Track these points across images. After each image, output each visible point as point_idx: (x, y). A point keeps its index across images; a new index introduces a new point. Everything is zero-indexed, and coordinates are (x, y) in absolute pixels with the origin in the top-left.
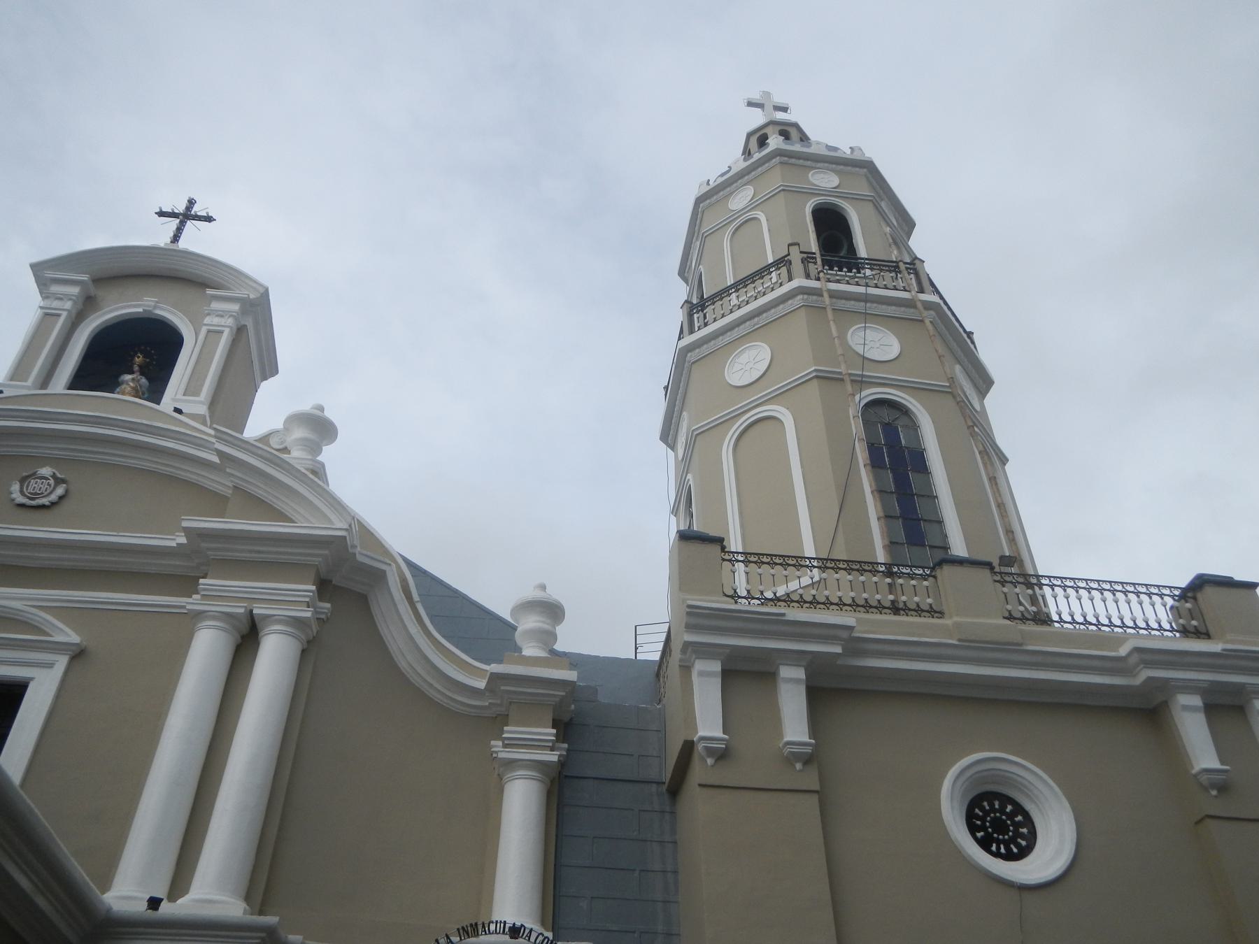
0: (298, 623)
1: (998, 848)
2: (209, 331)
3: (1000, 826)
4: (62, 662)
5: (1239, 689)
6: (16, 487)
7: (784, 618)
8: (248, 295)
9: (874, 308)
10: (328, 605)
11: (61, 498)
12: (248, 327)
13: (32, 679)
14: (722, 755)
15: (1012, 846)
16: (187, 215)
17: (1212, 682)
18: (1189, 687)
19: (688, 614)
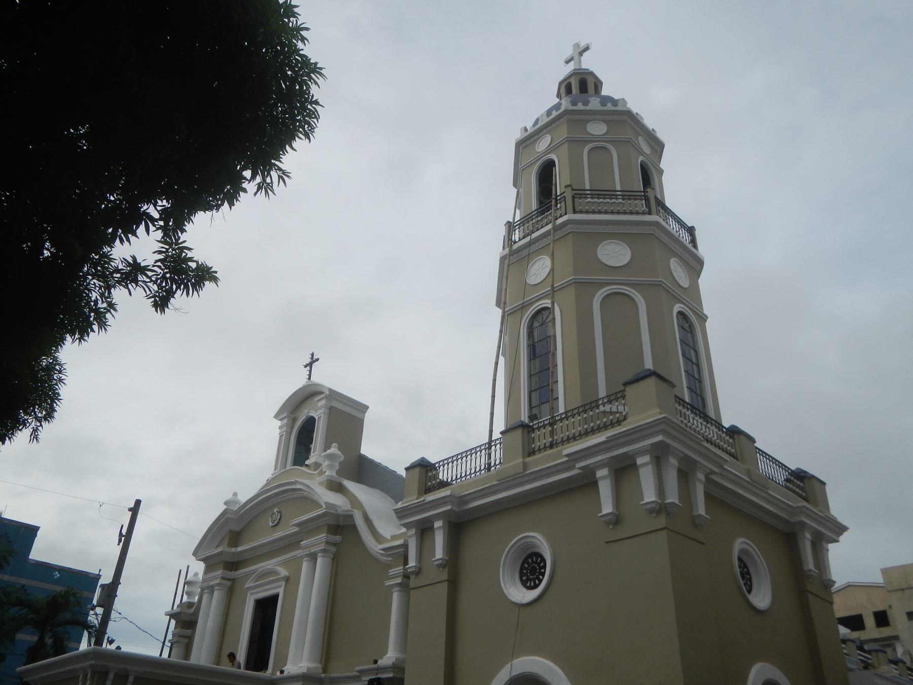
0: (324, 551)
1: (531, 584)
2: (319, 418)
3: (533, 571)
4: (283, 583)
5: (626, 456)
6: (270, 520)
7: (426, 501)
8: (326, 394)
9: (533, 248)
10: (338, 537)
11: (280, 519)
13: (279, 592)
14: (418, 572)
18: (600, 465)
19: (396, 513)
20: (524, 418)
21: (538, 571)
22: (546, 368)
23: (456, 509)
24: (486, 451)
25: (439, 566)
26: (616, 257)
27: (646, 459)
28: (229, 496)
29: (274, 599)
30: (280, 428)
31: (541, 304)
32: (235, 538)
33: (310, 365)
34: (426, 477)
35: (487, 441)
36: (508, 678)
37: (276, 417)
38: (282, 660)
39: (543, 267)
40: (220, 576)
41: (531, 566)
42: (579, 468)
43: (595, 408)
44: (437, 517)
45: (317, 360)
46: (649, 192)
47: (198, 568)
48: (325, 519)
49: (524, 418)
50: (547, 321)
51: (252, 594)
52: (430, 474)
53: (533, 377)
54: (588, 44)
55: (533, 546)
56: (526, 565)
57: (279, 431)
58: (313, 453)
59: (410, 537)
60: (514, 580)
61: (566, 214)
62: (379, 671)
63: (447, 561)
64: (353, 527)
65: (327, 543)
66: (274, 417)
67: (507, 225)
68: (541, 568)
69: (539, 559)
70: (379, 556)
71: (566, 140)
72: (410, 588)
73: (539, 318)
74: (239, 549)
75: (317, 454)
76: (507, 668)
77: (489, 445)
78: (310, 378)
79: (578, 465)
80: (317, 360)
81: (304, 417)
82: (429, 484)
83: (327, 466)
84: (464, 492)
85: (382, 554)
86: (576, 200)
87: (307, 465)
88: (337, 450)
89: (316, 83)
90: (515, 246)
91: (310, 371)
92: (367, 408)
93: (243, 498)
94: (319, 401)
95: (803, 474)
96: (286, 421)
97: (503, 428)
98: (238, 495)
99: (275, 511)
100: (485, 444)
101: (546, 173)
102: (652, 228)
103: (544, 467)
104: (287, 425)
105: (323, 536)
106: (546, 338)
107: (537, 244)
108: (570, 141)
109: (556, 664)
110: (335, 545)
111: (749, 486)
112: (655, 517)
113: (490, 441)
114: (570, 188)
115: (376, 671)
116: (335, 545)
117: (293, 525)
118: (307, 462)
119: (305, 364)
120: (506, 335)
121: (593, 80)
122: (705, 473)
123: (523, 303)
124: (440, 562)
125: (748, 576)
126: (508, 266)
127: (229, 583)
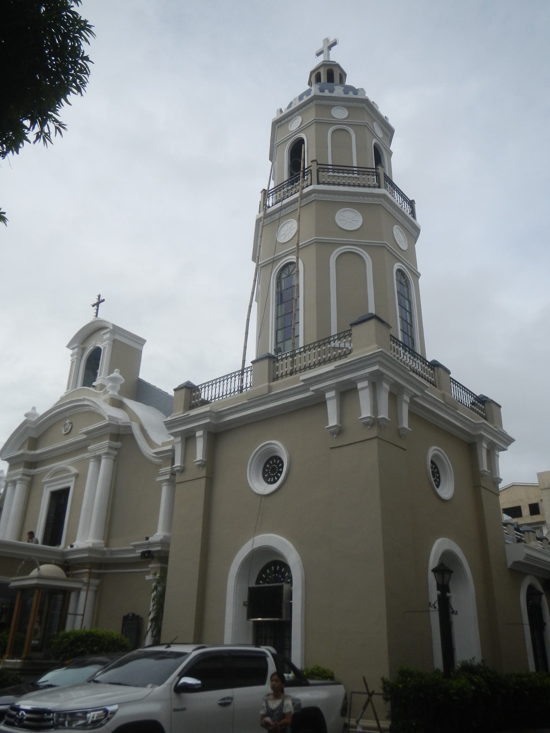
0: (107, 454)
1: (271, 479)
2: (104, 348)
3: (273, 470)
4: (74, 479)
6: (63, 429)
8: (110, 329)
9: (284, 212)
10: (119, 443)
11: (71, 429)
12: (117, 338)
14: (182, 470)
15: (276, 477)
16: (100, 301)
17: (337, 383)
18: (329, 389)
19: (165, 424)
20: (271, 351)
21: (277, 470)
22: (290, 312)
23: (215, 422)
24: (239, 376)
25: (199, 466)
26: (350, 222)
27: (365, 384)
28: (29, 410)
30: (72, 355)
31: (288, 259)
32: (34, 443)
33: (97, 304)
34: (191, 396)
35: (241, 369)
36: (250, 550)
37: (68, 346)
38: (72, 537)
39: (291, 229)
40: (22, 472)
41: (272, 466)
42: (313, 391)
43: (327, 344)
44: (199, 427)
45: (103, 301)
46: (380, 169)
48: (108, 429)
49: (271, 351)
50: (292, 273)
51: (48, 487)
52: (194, 394)
53: (279, 319)
54: (335, 39)
55: (274, 451)
56: (268, 466)
57: (70, 358)
58: (99, 376)
59: (177, 443)
60: (258, 477)
61: (311, 184)
62: (149, 546)
63: (205, 462)
64: (132, 436)
65: (110, 447)
66: (67, 347)
67: (263, 192)
68: (279, 468)
69: (278, 461)
70: (152, 458)
71: (314, 121)
72: (176, 482)
73: (286, 271)
74: (38, 452)
75: (102, 378)
76: (250, 542)
77: (242, 372)
78: (97, 316)
79: (311, 389)
80: (103, 301)
81: (92, 347)
82: (193, 402)
83: (110, 387)
84: (221, 408)
85: (154, 457)
86: (320, 173)
87: (94, 386)
88: (118, 374)
89: (86, 40)
90: (269, 211)
91: (97, 310)
92: (144, 341)
93: (40, 411)
94: (104, 334)
95: (485, 399)
96: (76, 350)
97: (254, 358)
98: (37, 409)
99: (67, 422)
100: (239, 371)
102: (381, 199)
103: (284, 389)
104: (77, 353)
105: (106, 442)
106: (291, 287)
107: (287, 209)
108: (318, 122)
109: (288, 540)
110: (116, 449)
111: (444, 408)
112: (369, 429)
113: (243, 369)
114: (315, 163)
115: (147, 546)
116: (116, 449)
117: (82, 434)
118: (94, 384)
119: (93, 304)
120: (259, 284)
121: (339, 72)
122: (410, 396)
123: (274, 258)
124: (200, 463)
125: (438, 475)
126: (263, 226)
127: (29, 479)
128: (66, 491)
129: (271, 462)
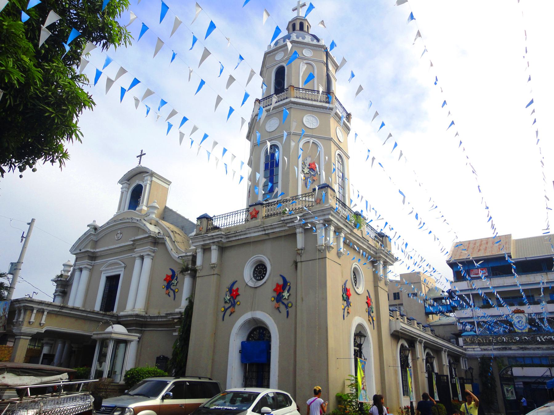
29: (118, 276)
32: (95, 243)
33: (141, 156)
38: (123, 306)
45: (145, 154)
47: (72, 258)
51: (104, 273)
52: (210, 222)
54: (305, 3)
56: (257, 269)
57: (121, 190)
68: (264, 271)
74: (97, 250)
78: (140, 163)
79: (288, 225)
80: (145, 154)
91: (140, 160)
95: (383, 235)
101: (280, 73)
111: (361, 240)
117: (131, 241)
121: (307, 24)
128: (118, 276)
129: (259, 267)
